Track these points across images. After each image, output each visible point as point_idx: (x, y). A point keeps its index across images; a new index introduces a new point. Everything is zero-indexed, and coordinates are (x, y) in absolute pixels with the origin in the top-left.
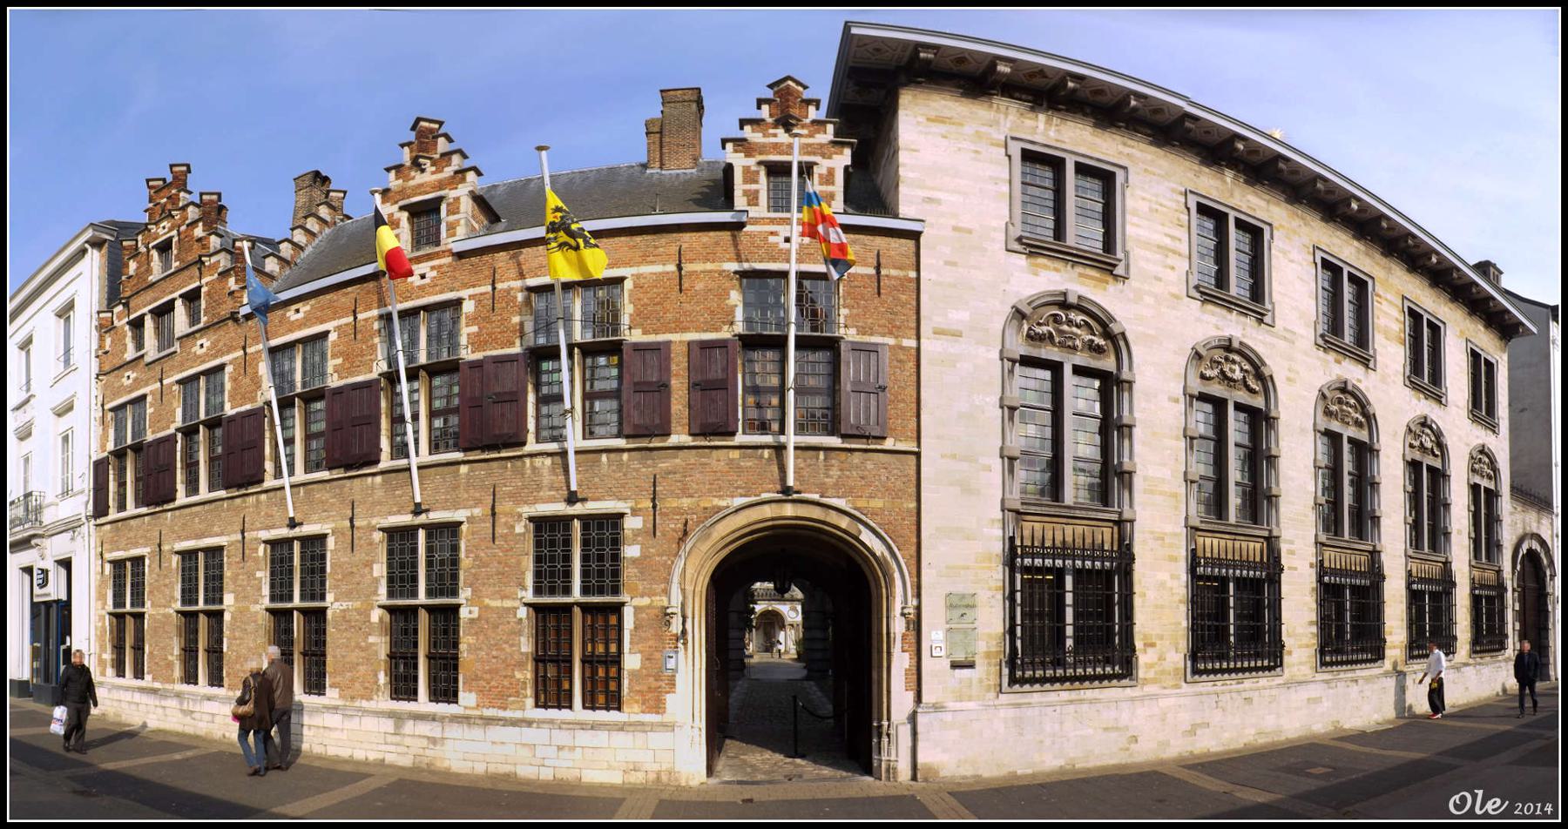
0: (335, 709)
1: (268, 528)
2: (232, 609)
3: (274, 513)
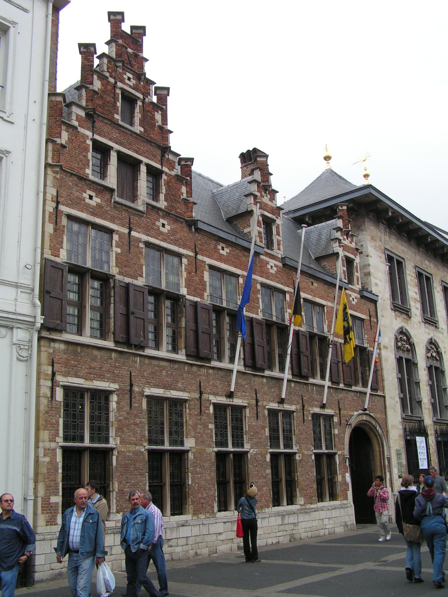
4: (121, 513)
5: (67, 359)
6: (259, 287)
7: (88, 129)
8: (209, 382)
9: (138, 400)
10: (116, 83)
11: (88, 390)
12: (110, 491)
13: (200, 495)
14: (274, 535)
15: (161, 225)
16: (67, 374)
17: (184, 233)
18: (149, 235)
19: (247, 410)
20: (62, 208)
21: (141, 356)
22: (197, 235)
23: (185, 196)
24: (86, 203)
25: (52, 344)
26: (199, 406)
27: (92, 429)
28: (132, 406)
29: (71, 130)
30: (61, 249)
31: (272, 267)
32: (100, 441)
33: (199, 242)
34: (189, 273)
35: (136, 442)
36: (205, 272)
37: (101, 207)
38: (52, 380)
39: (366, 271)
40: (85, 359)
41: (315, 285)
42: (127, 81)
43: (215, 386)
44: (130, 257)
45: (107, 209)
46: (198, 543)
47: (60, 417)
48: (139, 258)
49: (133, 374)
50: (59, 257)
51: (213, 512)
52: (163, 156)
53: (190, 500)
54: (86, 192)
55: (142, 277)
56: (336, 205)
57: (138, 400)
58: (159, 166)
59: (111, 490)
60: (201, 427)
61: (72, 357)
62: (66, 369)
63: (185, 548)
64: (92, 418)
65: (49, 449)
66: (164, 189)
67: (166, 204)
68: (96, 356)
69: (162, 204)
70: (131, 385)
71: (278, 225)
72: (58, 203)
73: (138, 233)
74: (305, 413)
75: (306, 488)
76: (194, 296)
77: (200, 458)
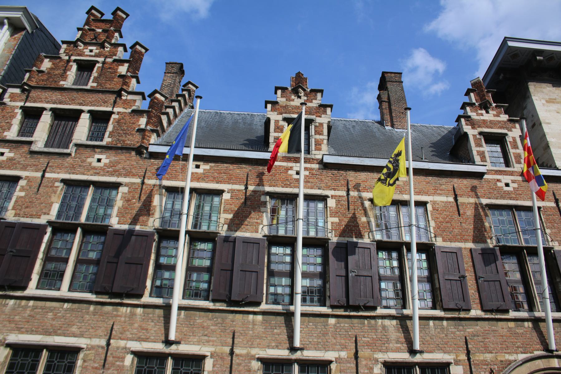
3: (149, 327)
43: (143, 329)
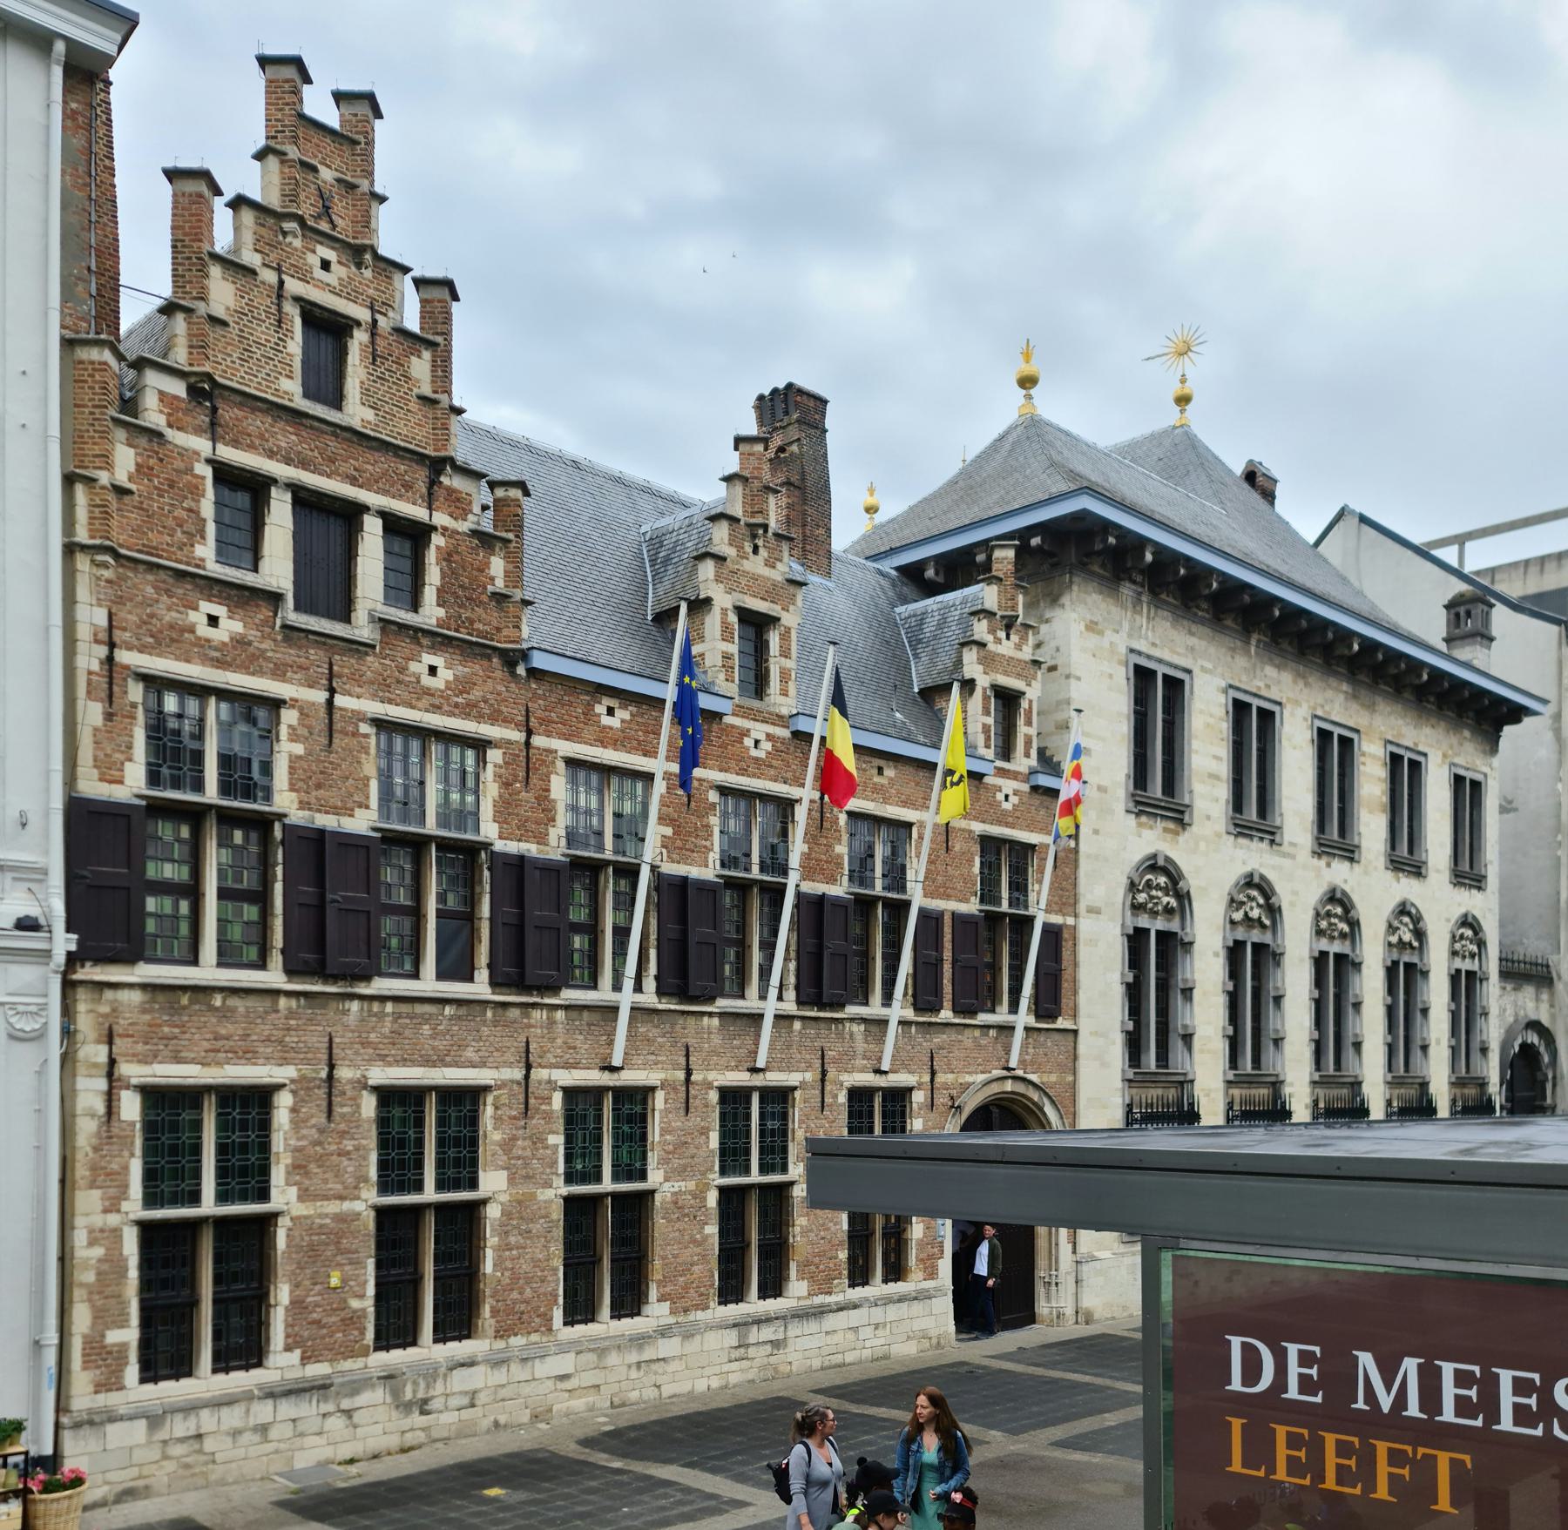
0: (664, 1332)
1: (568, 1066)
2: (504, 1198)
3: (578, 1044)
4: (297, 1353)
5: (150, 1025)
6: (713, 796)
7: (198, 431)
8: (553, 1040)
9: (350, 1099)
10: (281, 283)
11: (208, 1089)
12: (270, 1306)
13: (515, 1295)
14: (717, 1369)
15: (426, 670)
16: (144, 1060)
17: (491, 682)
18: (390, 701)
19: (660, 1097)
20: (124, 657)
21: (362, 998)
22: (534, 686)
23: (500, 584)
24: (199, 638)
25: (109, 994)
26: (521, 1098)
27: (222, 1173)
28: (334, 1113)
29: (143, 441)
30: (127, 764)
31: (757, 742)
32: (244, 1197)
33: (541, 702)
34: (507, 785)
35: (345, 1193)
36: (553, 777)
37: (245, 643)
38: (110, 1075)
39: (1060, 716)
40: (202, 1019)
41: (890, 772)
42: (319, 273)
43: (570, 1048)
44: (331, 763)
45: (263, 646)
46: (503, 1400)
47: (132, 1155)
48: (359, 762)
49: (337, 1040)
50: (121, 782)
51: (550, 1330)
52: (433, 483)
53: (486, 1311)
54: (196, 609)
55: (367, 807)
56: (986, 545)
57: (350, 1099)
58: (419, 512)
59: (272, 1302)
60: (527, 1143)
61: (166, 1018)
62: (148, 1047)
63: (467, 1414)
64: (222, 1149)
65: (102, 1231)
66: (433, 575)
67: (441, 612)
68: (233, 1010)
69: (431, 613)
70: (332, 1067)
71: (788, 630)
72: (112, 645)
73: (355, 700)
74: (828, 1088)
75: (817, 1260)
76: (520, 840)
77: (519, 1212)
